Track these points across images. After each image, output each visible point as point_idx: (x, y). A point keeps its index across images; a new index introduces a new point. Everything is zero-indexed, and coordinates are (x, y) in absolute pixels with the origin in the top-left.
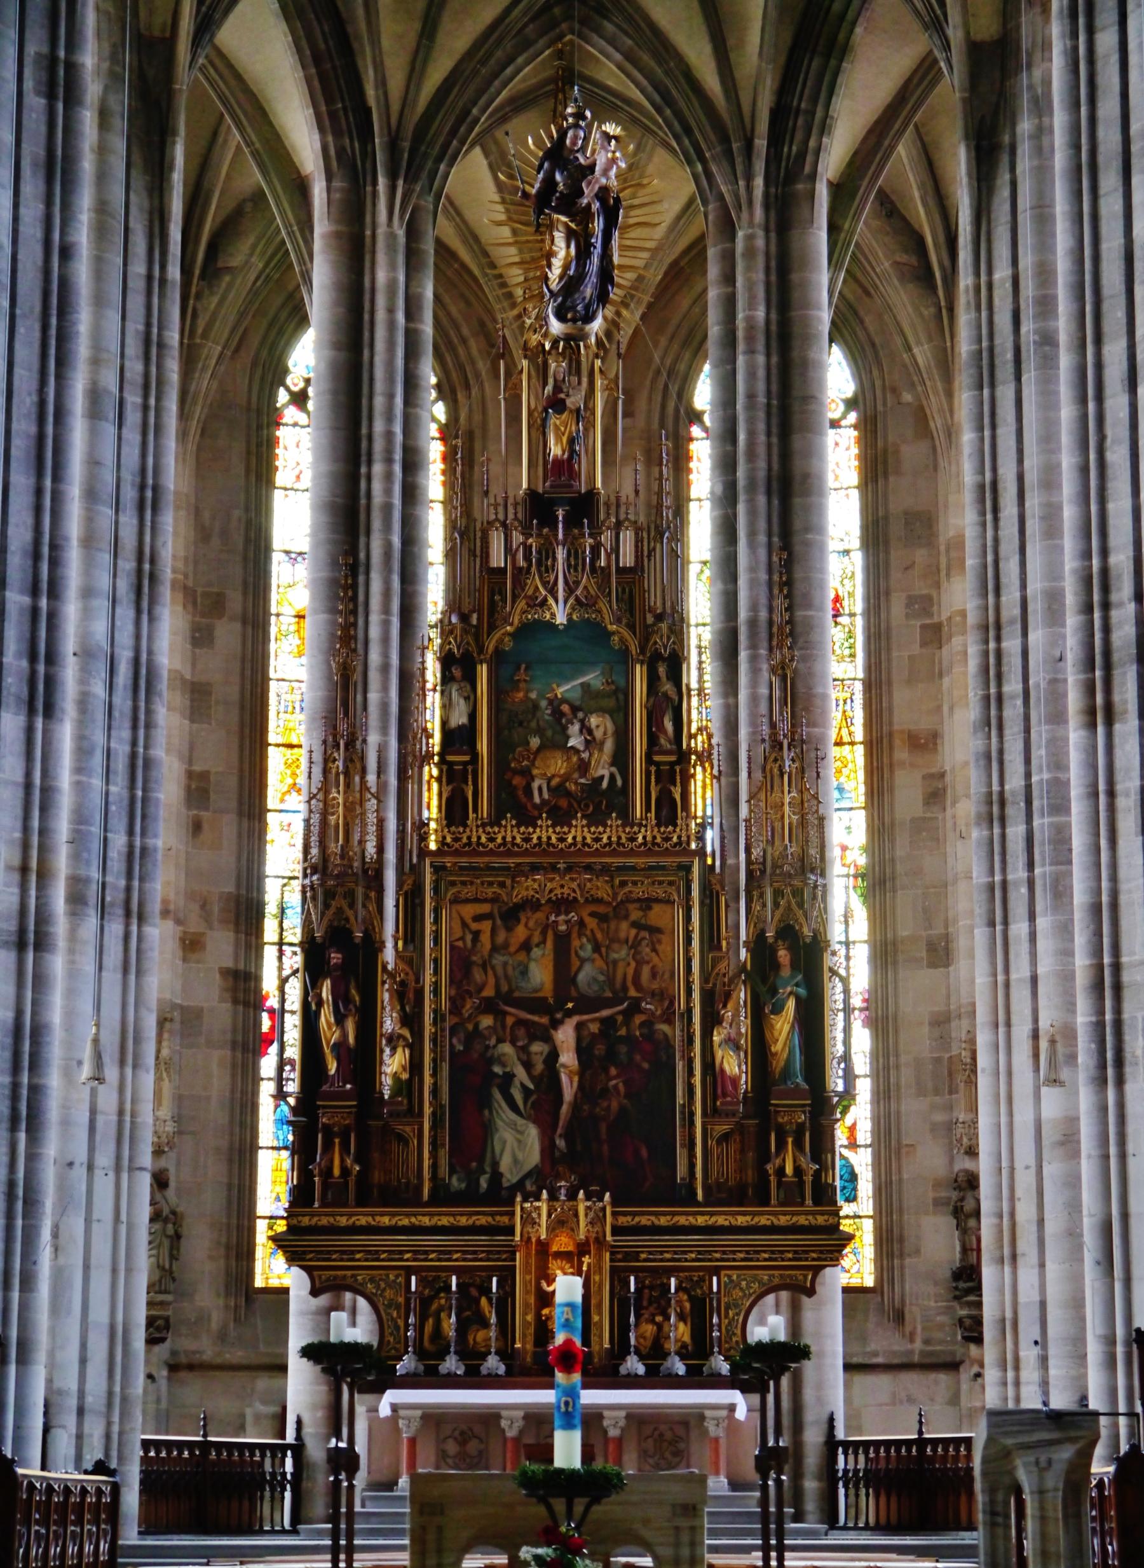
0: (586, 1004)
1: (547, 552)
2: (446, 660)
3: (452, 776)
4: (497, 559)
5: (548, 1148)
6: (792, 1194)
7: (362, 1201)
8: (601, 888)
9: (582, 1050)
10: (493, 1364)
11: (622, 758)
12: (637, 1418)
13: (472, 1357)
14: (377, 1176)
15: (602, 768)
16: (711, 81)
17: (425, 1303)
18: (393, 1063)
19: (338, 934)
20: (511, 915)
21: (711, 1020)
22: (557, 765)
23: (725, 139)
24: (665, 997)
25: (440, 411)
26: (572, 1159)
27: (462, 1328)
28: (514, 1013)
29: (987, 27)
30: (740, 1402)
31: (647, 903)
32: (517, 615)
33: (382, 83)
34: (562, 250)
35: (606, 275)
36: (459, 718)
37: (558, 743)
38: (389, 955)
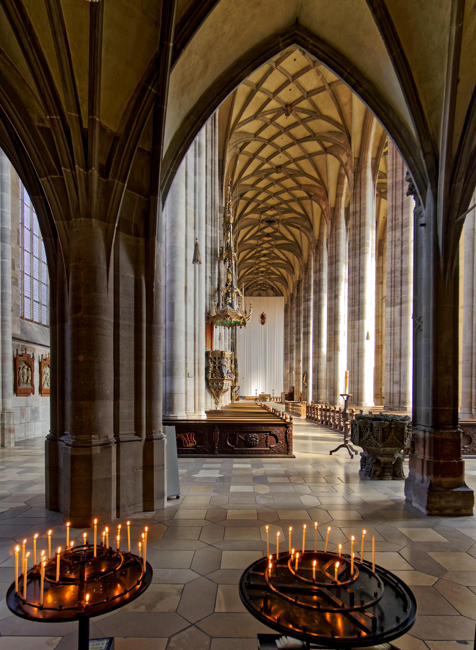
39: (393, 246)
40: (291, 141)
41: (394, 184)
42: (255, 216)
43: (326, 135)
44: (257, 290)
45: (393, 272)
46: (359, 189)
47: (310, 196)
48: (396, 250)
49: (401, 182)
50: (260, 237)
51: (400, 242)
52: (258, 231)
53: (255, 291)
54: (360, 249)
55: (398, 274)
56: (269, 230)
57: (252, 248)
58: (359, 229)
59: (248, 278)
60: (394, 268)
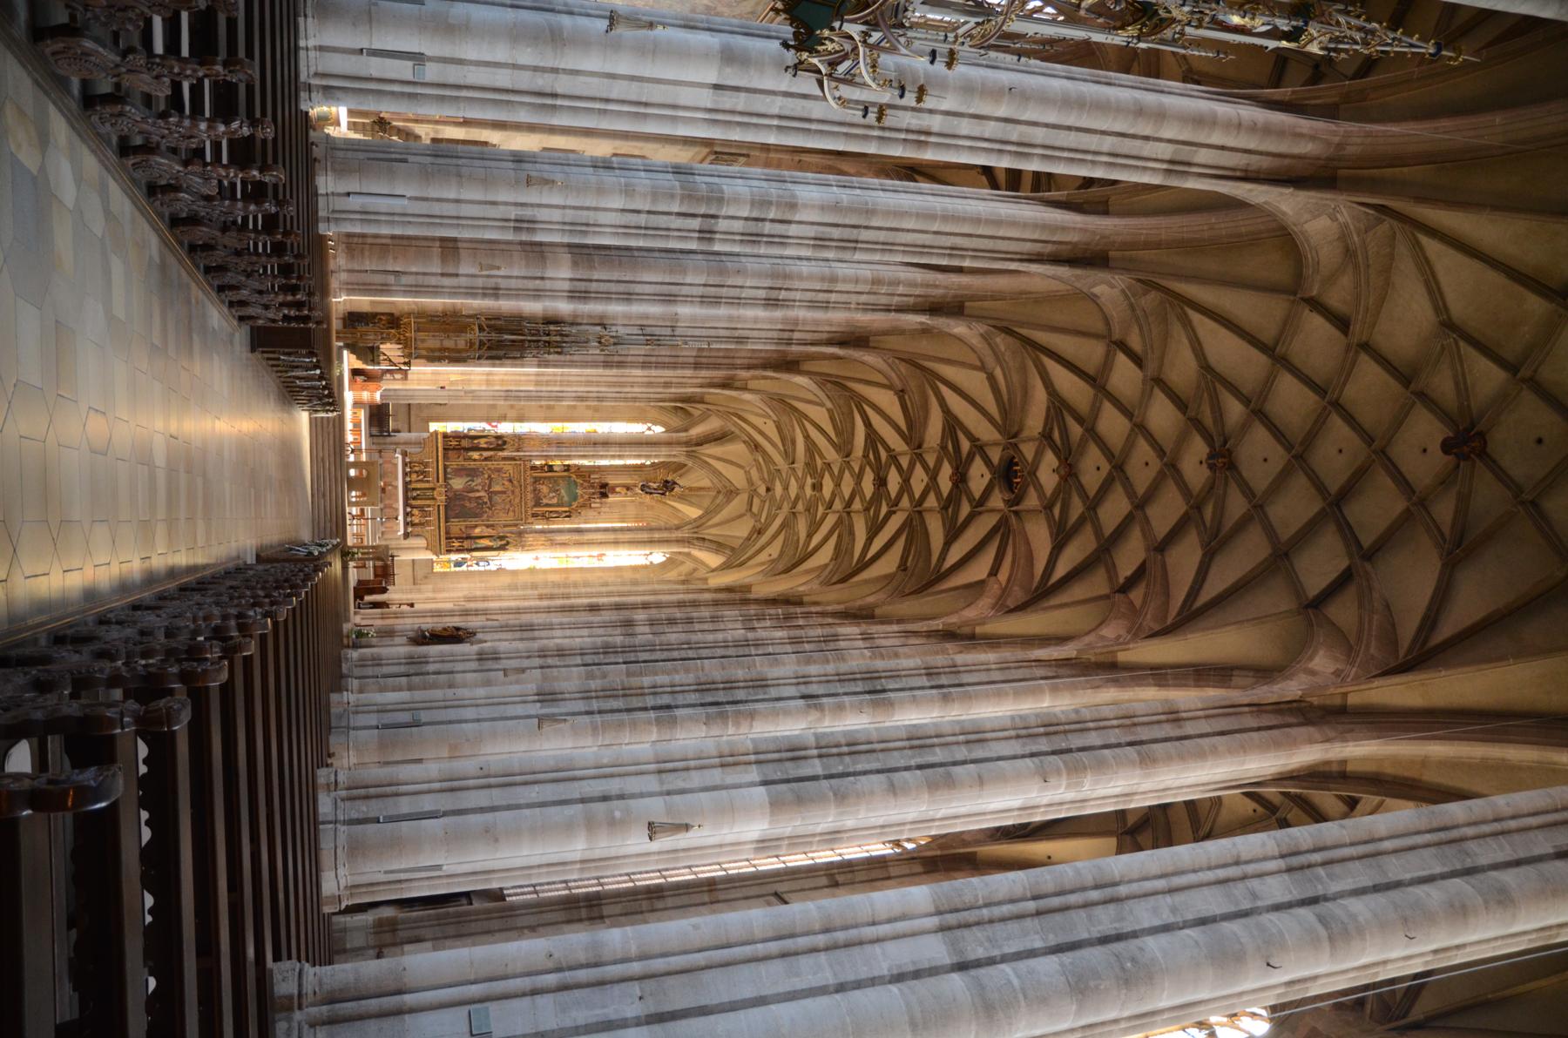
0: (490, 499)
1: (593, 487)
8: (517, 500)
10: (408, 479)
11: (547, 505)
15: (545, 501)
16: (710, 523)
18: (475, 455)
19: (505, 443)
20: (510, 481)
21: (488, 526)
25: (648, 463)
30: (401, 532)
32: (579, 481)
38: (500, 453)
39: (1221, 873)
40: (1334, 487)
41: (1455, 834)
42: (1035, 421)
43: (1376, 595)
44: (750, 481)
45: (1108, 892)
46: (1255, 725)
48: (1206, 891)
49: (1469, 863)
51: (1246, 905)
52: (972, 439)
53: (747, 473)
54: (1054, 753)
55: (1105, 920)
56: (979, 476)
58: (1124, 740)
59: (794, 442)
60: (1128, 898)
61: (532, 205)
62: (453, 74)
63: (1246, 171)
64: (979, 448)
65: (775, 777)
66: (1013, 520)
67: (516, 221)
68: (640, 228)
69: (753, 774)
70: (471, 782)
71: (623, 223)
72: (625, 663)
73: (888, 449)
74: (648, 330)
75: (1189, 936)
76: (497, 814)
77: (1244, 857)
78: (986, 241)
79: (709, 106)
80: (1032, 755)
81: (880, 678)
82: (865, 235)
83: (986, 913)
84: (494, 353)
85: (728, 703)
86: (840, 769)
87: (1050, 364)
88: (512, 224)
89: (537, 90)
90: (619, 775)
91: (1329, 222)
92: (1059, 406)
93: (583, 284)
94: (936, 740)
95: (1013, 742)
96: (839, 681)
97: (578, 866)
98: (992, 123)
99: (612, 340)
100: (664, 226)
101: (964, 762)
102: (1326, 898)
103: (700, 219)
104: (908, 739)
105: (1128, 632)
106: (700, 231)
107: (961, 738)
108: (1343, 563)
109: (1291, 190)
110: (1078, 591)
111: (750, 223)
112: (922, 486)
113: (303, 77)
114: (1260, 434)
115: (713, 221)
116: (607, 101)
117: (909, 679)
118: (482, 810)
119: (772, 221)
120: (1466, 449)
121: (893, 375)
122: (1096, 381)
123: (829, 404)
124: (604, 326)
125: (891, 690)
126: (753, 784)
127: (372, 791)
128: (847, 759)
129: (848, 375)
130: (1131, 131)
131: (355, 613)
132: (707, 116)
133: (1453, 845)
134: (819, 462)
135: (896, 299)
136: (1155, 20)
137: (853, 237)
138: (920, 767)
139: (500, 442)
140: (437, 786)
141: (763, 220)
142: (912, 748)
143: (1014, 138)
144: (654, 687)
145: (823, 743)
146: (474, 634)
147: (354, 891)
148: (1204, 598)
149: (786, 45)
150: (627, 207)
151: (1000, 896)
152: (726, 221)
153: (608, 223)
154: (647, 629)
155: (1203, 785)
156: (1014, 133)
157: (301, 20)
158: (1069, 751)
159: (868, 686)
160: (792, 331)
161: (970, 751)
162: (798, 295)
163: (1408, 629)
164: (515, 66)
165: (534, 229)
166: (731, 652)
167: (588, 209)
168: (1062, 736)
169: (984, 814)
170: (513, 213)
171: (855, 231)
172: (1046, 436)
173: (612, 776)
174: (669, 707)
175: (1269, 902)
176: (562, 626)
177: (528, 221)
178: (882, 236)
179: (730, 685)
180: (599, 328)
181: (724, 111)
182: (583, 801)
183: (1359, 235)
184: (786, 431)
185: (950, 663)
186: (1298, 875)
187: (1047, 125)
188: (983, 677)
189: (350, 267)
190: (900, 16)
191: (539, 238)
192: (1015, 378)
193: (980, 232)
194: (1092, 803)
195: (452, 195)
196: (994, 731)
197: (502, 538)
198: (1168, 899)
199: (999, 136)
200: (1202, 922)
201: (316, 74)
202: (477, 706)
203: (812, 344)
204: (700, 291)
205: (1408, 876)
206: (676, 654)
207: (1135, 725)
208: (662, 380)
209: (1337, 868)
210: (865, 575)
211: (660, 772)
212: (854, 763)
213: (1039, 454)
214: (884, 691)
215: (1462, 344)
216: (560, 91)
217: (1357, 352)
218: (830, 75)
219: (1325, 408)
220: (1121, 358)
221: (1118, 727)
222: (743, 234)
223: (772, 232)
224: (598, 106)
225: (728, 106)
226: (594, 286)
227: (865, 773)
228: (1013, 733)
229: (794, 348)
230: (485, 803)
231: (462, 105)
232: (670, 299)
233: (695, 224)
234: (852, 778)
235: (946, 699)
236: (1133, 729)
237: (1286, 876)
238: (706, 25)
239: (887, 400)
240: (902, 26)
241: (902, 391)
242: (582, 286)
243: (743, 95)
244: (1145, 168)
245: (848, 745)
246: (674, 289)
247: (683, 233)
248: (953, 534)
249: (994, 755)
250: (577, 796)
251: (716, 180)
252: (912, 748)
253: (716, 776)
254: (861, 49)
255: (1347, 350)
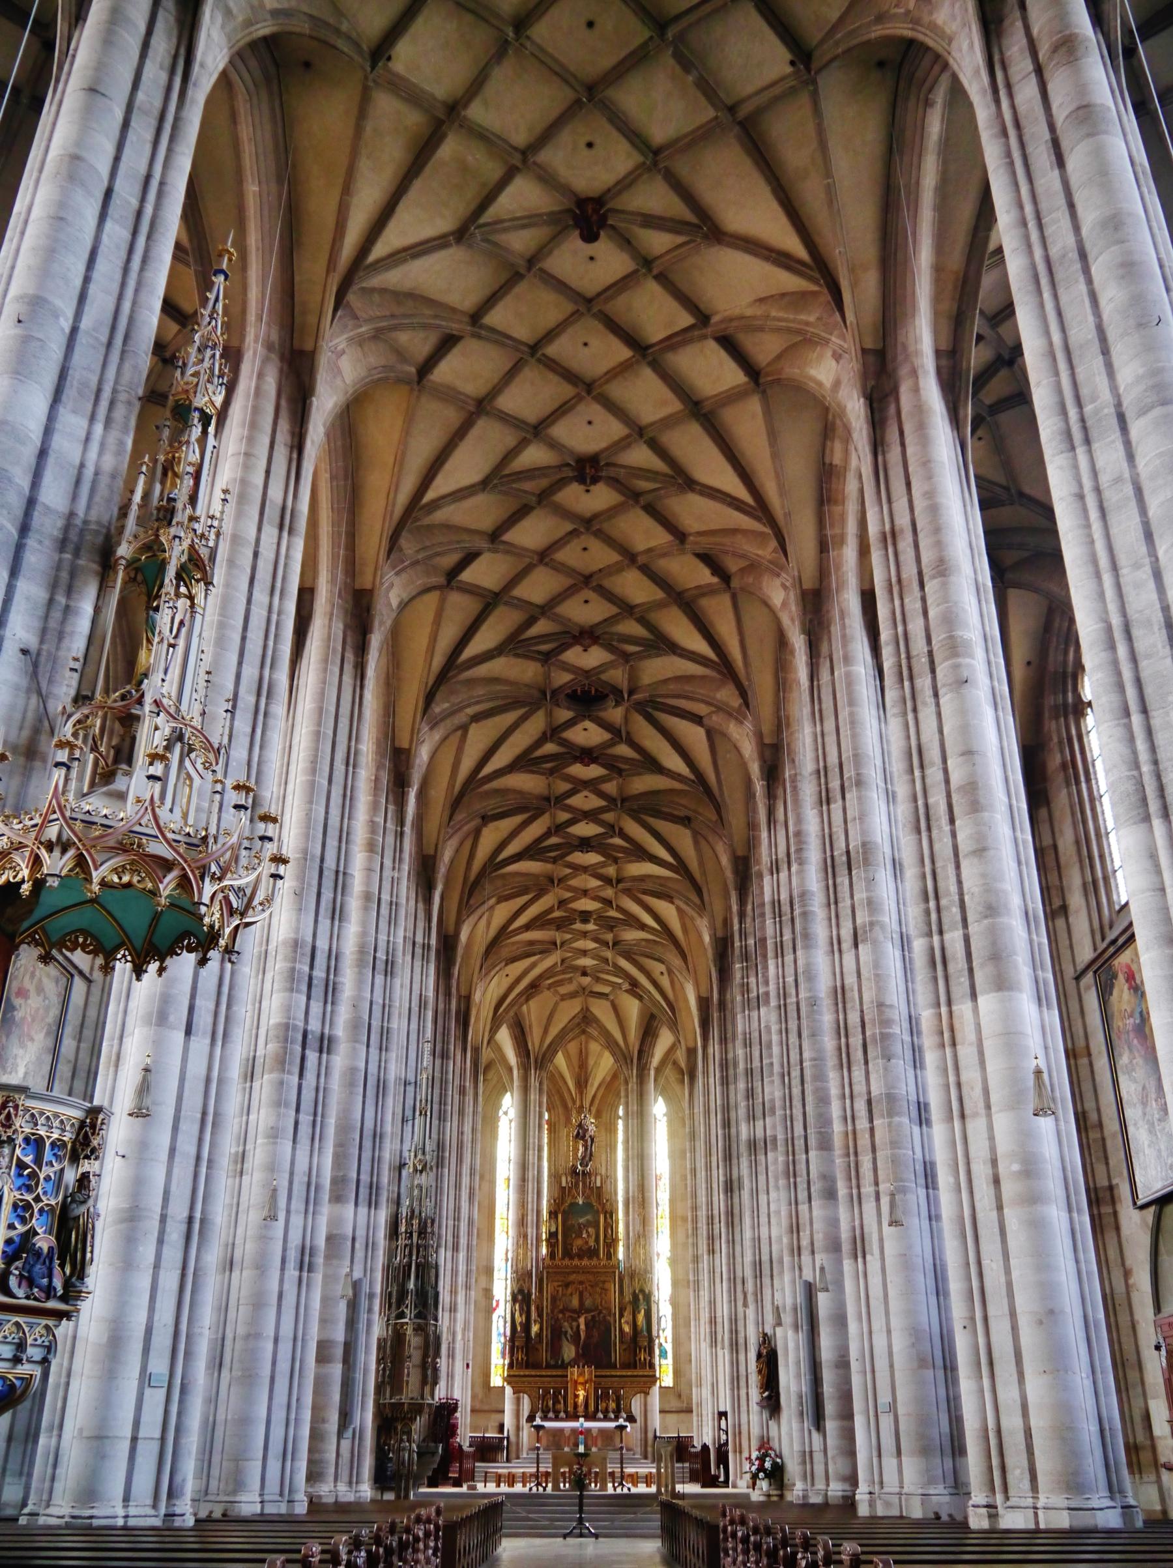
0: (588, 1311)
1: (577, 1184)
2: (550, 1213)
3: (551, 1245)
4: (564, 1184)
5: (577, 1352)
6: (643, 1366)
7: (527, 1367)
8: (591, 1277)
9: (586, 1325)
10: (562, 1415)
12: (602, 1431)
13: (557, 1412)
14: (531, 1360)
15: (592, 1243)
16: (621, 1042)
17: (544, 1396)
18: (535, 1329)
19: (521, 1291)
20: (567, 1285)
21: (621, 1316)
22: (579, 1242)
23: (625, 1059)
24: (609, 1309)
26: (584, 1355)
27: (554, 1404)
28: (568, 1314)
29: (691, 1045)
31: (604, 1282)
32: (569, 1201)
33: (533, 1044)
34: (581, 1149)
35: (591, 1155)
36: (553, 1229)
37: (580, 1235)
39: (1094, 514)
42: (524, 671)
43: (749, 312)
44: (573, 995)
45: (1118, 635)
47: (725, 577)
48: (1114, 531)
50: (555, 765)
51: (1129, 490)
53: (563, 998)
56: (588, 734)
57: (532, 807)
59: (531, 943)
61: (285, 1250)
62: (162, 1340)
63: (292, 448)
64: (553, 732)
65: (967, 983)
66: (637, 697)
67: (301, 1269)
68: (314, 1122)
69: (963, 1009)
70: (981, 1340)
71: (308, 1142)
72: (807, 1152)
73: (548, 834)
74: (409, 1113)
75: (1166, 551)
76: (1018, 1310)
77: (1074, 489)
78: (340, 725)
79: (208, 1041)
80: (936, 695)
81: (832, 857)
82: (330, 863)
83: (1146, 768)
84: (431, 1301)
85: (864, 1032)
86: (956, 910)
87: (469, 652)
88: (305, 1274)
89: (182, 1242)
90: (968, 1164)
91: (344, 357)
92: (513, 645)
93: (361, 1190)
94: (920, 802)
95: (921, 716)
96: (836, 903)
97: (1075, 1215)
98: (236, 723)
99: (420, 1156)
100: (313, 1094)
101: (946, 771)
102: (1119, 405)
103: (307, 1052)
104: (919, 832)
105: (778, 575)
106: (321, 1051)
107: (917, 773)
108: (712, 345)
109: (314, 399)
110: (726, 629)
111: (313, 994)
112: (592, 796)
113: (157, 1522)
114: (561, 431)
115: (310, 1037)
116: (198, 1158)
117: (834, 824)
118: (1015, 1328)
119: (312, 967)
120: (595, 218)
121: (466, 828)
122: (490, 601)
123: (493, 901)
124: (402, 1166)
125: (847, 845)
126: (976, 1010)
127: (995, 1462)
128: (944, 902)
129: (461, 880)
130: (249, 571)
131: (734, 1486)
132: (219, 1043)
133: (1054, 270)
134: (557, 914)
135: (390, 825)
136: (190, 567)
137: (333, 877)
138: (952, 821)
139: (520, 1297)
140: (986, 1382)
141: (310, 978)
142: (929, 829)
143: (253, 699)
144: (845, 1119)
145: (926, 929)
146: (765, 1335)
147: (1116, 1488)
148: (743, 494)
149: (203, 962)
150: (291, 1137)
151: (1126, 751)
152: (311, 1021)
153: (307, 1160)
154: (759, 1124)
155: (965, 506)
156: (247, 699)
157: (96, 1522)
158: (930, 653)
159: (842, 870)
160: (414, 943)
161: (932, 764)
162: (383, 938)
163: (790, 282)
164: (157, 1266)
165: (311, 1248)
166: (793, 1025)
167: (291, 1183)
168: (914, 661)
169: (1002, 748)
170: (292, 1273)
171: (326, 873)
172: (547, 658)
173: (969, 1172)
174: (869, 1102)
175: (1125, 465)
176: (756, 1226)
177: (303, 1254)
178: (332, 843)
179: (842, 1030)
180: (404, 1173)
181: (215, 1024)
182: (1000, 1208)
183: (361, 326)
184: (519, 952)
185: (814, 777)
186: (1094, 434)
187: (240, 663)
188: (831, 740)
189: (331, 1478)
190: (195, 841)
191: (321, 1242)
192: (480, 691)
193: (330, 733)
194: (987, 629)
195: (270, 1346)
196: (908, 737)
197: (635, 1297)
198: (1124, 572)
199: (250, 716)
200: (1149, 536)
201: (155, 1506)
202: (870, 1333)
203: (430, 921)
204: (374, 1051)
205: (1091, 319)
206: (796, 1091)
207: (899, 581)
208: (456, 1097)
209: (1084, 392)
210: (694, 866)
211: (963, 1116)
212: (948, 894)
213: (567, 667)
214: (848, 852)
215: (482, 220)
216: (185, 1214)
217: (482, 327)
218: (243, 914)
219: (539, 361)
220: (466, 576)
221: (902, 599)
222: (325, 1002)
223: (324, 967)
224: (203, 1170)
225: (210, 1020)
226: (365, 1177)
227: (960, 882)
228: (910, 716)
229: (433, 942)
230: (1006, 1325)
231: (197, 1330)
232: (381, 1087)
233: (312, 1056)
234: (967, 898)
235: (859, 783)
236: (905, 583)
237: (1095, 446)
238: (116, 1042)
239: (490, 837)
240: (205, 839)
241: (483, 818)
242: (363, 1192)
243: (198, 1002)
244: (287, 556)
245: (927, 900)
246: (372, 1082)
247: (324, 1071)
248: (652, 765)
249: (937, 736)
250: (995, 1213)
251: (262, 1032)
252: (929, 829)
253: (967, 1052)
254: (226, 883)
255: (479, 337)
